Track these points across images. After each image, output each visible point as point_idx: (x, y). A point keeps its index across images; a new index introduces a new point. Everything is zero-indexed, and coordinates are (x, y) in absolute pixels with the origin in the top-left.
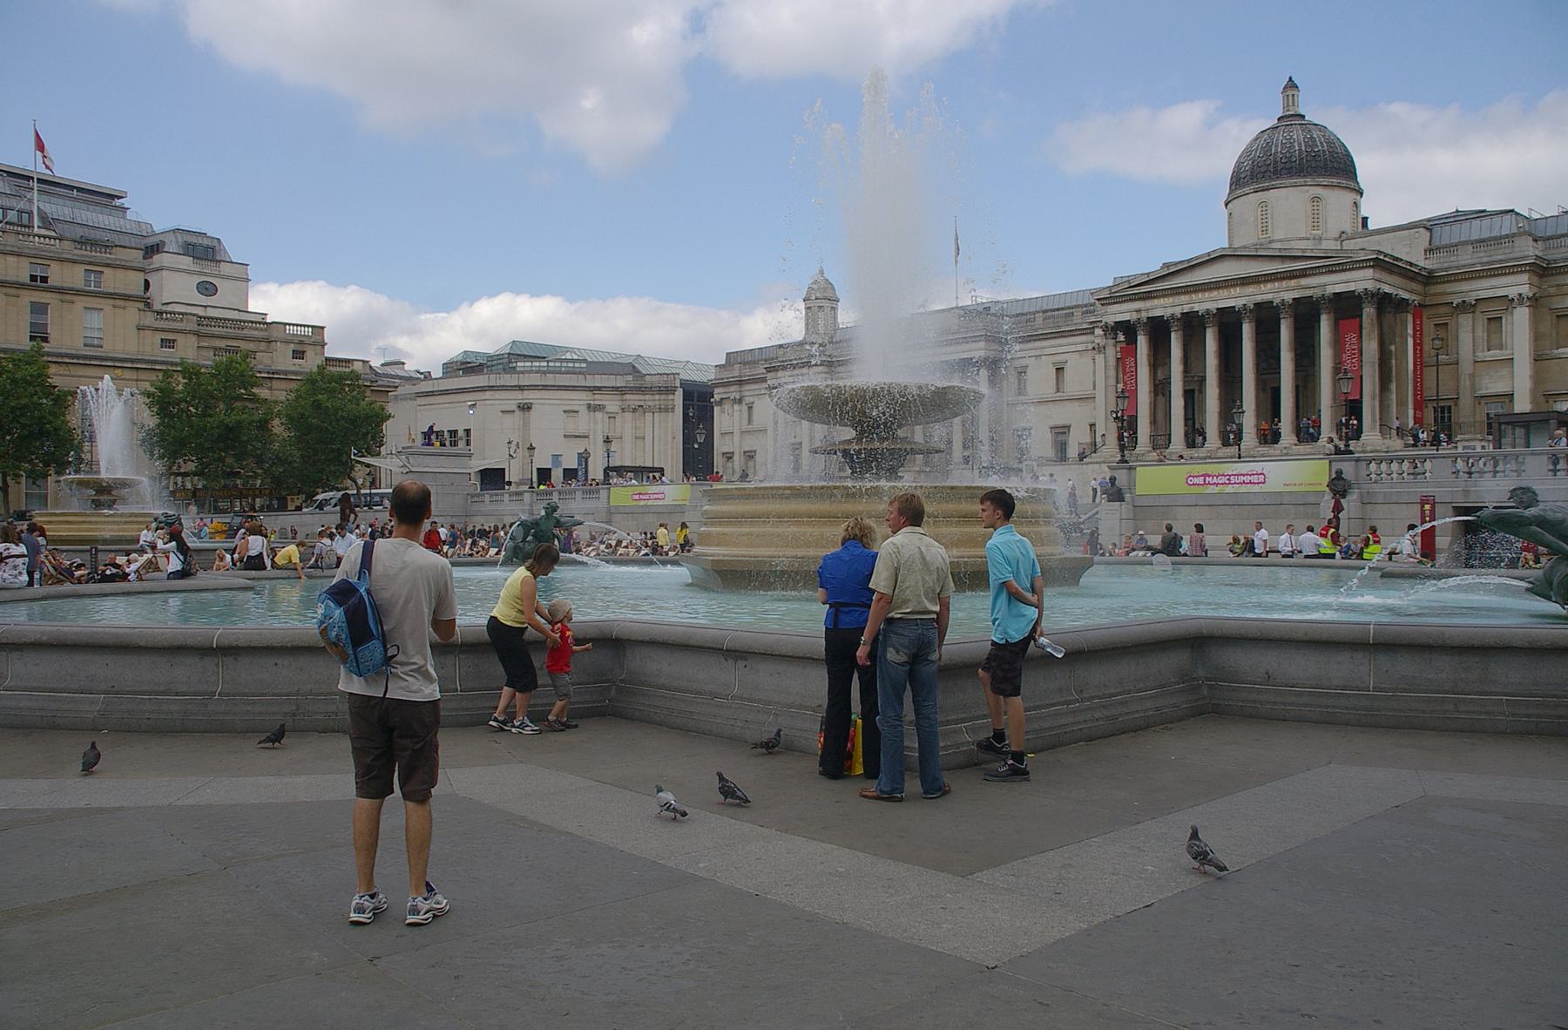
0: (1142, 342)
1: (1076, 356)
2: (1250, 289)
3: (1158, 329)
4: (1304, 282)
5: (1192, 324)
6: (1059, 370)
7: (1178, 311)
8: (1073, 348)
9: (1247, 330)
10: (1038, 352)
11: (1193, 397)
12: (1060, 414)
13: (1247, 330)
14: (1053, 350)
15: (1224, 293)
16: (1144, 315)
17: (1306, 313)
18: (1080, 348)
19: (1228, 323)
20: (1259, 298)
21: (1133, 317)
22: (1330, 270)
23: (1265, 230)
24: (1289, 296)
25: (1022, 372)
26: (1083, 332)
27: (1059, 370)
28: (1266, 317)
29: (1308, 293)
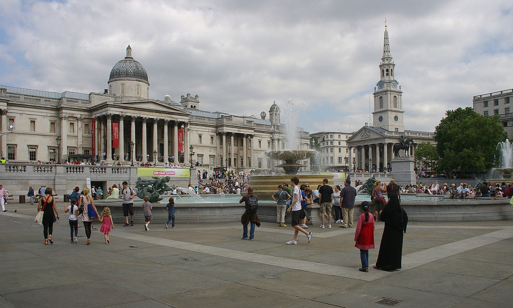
0: (122, 123)
1: (42, 117)
2: (157, 114)
3: (128, 120)
4: (172, 116)
5: (139, 121)
6: (33, 122)
7: (136, 116)
8: (40, 114)
9: (156, 126)
10: (22, 112)
11: (161, 147)
12: (33, 141)
13: (156, 126)
14: (33, 113)
15: (151, 113)
16: (124, 114)
17: (172, 124)
18: (43, 114)
19: (150, 123)
20: (160, 118)
21: (120, 114)
22: (179, 114)
23: (138, 94)
24: (169, 119)
25: (12, 120)
26: (46, 108)
27: (33, 122)
28: (161, 123)
29: (173, 119)
